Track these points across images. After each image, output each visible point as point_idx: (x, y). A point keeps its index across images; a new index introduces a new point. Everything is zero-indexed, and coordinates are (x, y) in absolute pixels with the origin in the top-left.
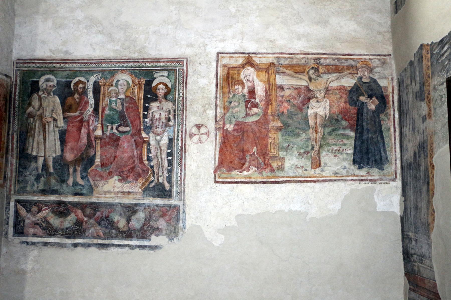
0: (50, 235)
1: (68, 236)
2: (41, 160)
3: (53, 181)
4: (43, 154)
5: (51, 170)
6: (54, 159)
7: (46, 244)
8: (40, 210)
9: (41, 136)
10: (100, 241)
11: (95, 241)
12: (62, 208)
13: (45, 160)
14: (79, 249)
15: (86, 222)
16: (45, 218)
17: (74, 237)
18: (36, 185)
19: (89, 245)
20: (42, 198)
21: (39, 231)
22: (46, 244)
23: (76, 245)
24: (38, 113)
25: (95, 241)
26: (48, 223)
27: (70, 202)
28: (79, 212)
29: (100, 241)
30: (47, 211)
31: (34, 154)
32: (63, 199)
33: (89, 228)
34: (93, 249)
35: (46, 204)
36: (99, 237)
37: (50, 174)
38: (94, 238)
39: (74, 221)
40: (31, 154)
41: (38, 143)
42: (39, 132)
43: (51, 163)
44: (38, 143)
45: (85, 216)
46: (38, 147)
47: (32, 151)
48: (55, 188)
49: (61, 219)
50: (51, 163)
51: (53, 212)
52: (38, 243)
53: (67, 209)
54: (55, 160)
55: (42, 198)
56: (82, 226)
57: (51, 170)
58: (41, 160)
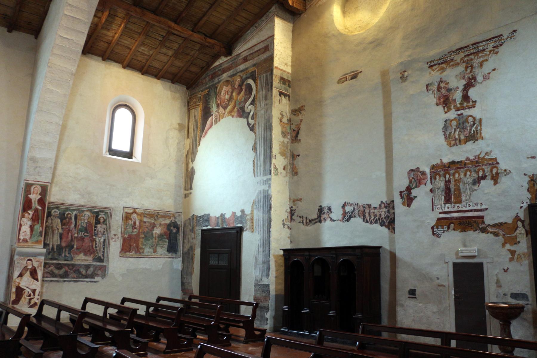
0: (54, 277)
1: (61, 278)
2: (51, 246)
3: (55, 255)
4: (52, 243)
5: (55, 250)
6: (57, 245)
7: (51, 281)
8: (50, 267)
9: (52, 235)
10: (75, 279)
11: (73, 279)
12: (59, 266)
13: (53, 246)
14: (66, 282)
15: (69, 272)
16: (52, 270)
17: (64, 278)
18: (48, 256)
19: (70, 281)
20: (50, 262)
21: (49, 275)
22: (51, 281)
23: (64, 281)
24: (51, 225)
25: (73, 279)
26: (53, 272)
27: (63, 264)
28: (67, 267)
29: (75, 279)
30: (53, 267)
31: (48, 243)
32: (60, 262)
33: (70, 274)
34: (72, 283)
35: (52, 264)
36: (74, 278)
37: (54, 252)
38: (72, 278)
39: (64, 271)
40: (47, 243)
41: (50, 238)
42: (51, 234)
43: (55, 247)
44: (50, 238)
45: (69, 269)
46: (50, 240)
47: (47, 242)
48: (57, 257)
49: (59, 271)
50: (55, 247)
51: (55, 267)
52: (48, 280)
53: (62, 266)
54: (57, 246)
55: (50, 262)
56: (67, 273)
57: (55, 250)
58: (51, 246)
